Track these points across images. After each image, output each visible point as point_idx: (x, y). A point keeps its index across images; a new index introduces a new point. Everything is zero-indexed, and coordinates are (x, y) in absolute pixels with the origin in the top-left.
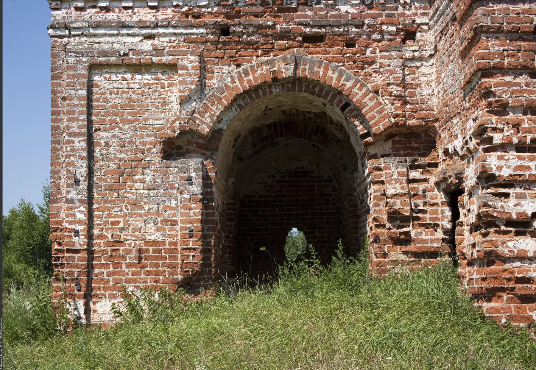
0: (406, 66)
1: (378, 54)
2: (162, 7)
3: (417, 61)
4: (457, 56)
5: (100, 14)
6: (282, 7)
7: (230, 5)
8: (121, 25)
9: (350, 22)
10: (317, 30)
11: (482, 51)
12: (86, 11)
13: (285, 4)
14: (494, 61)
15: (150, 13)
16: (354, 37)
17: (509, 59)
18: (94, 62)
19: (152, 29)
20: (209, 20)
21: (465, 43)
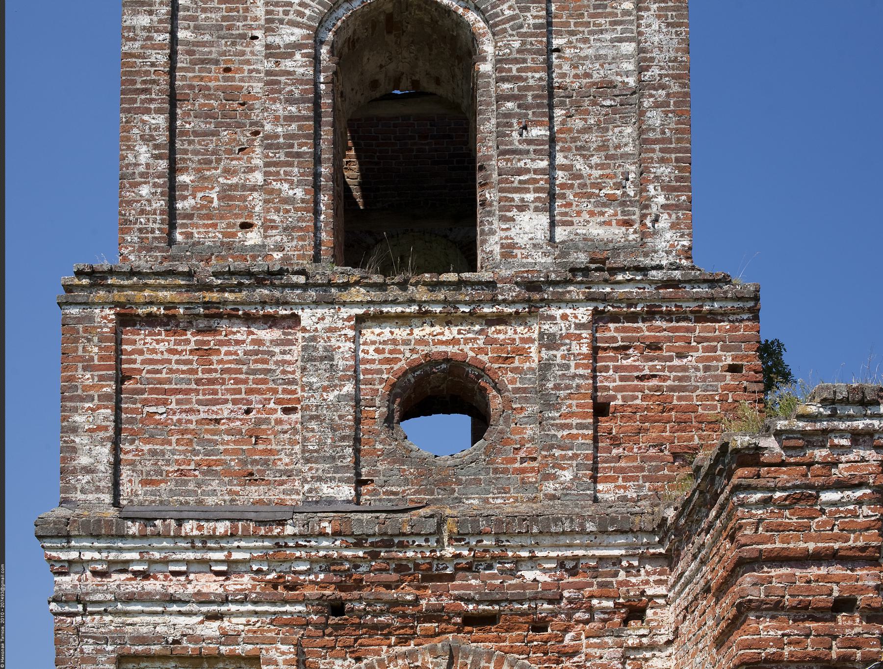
0: (628, 658)
1: (584, 641)
2: (235, 573)
3: (646, 651)
4: (709, 644)
5: (133, 582)
6: (430, 573)
7: (345, 571)
8: (168, 599)
9: (540, 596)
10: (486, 607)
11: (749, 637)
12: (110, 577)
13: (434, 569)
14: (768, 651)
15: (215, 581)
16: (546, 617)
17: (792, 648)
18: (126, 652)
19: (219, 606)
20: (311, 592)
21: (723, 624)
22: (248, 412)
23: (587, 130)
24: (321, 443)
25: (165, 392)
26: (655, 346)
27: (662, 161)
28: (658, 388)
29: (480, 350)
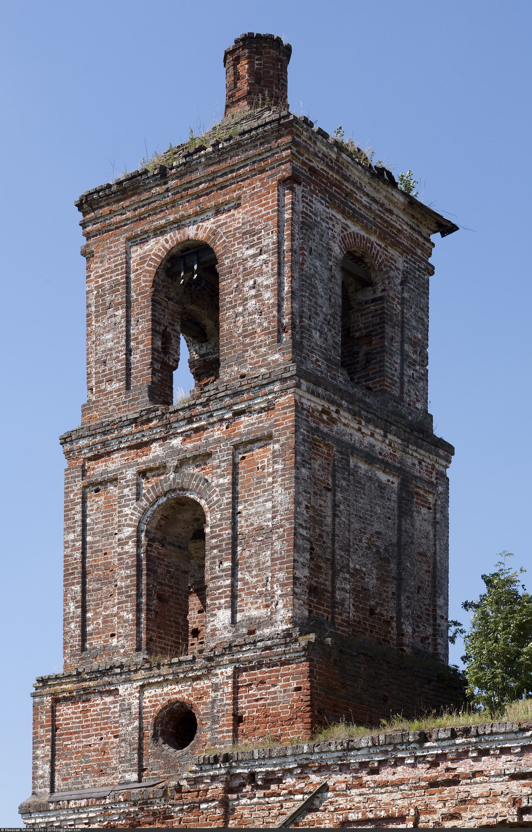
22: (101, 739)
23: (251, 556)
24: (126, 753)
25: (71, 734)
26: (263, 682)
27: (280, 570)
28: (264, 705)
29: (190, 695)
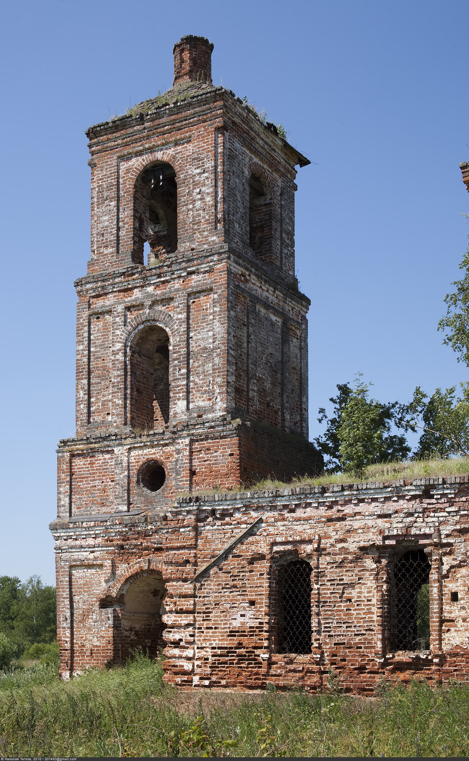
20: (115, 543)
